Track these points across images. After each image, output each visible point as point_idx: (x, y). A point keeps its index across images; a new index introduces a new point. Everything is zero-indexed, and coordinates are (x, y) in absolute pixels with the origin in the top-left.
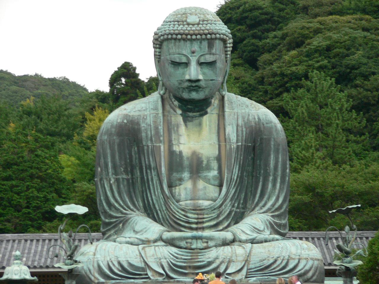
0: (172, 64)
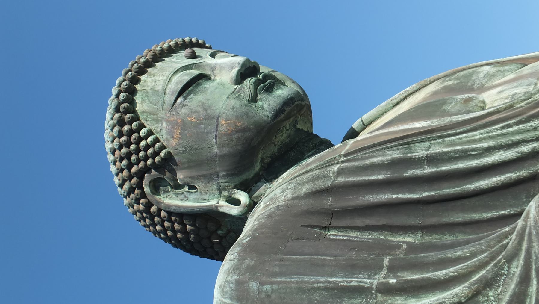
0: (185, 98)
